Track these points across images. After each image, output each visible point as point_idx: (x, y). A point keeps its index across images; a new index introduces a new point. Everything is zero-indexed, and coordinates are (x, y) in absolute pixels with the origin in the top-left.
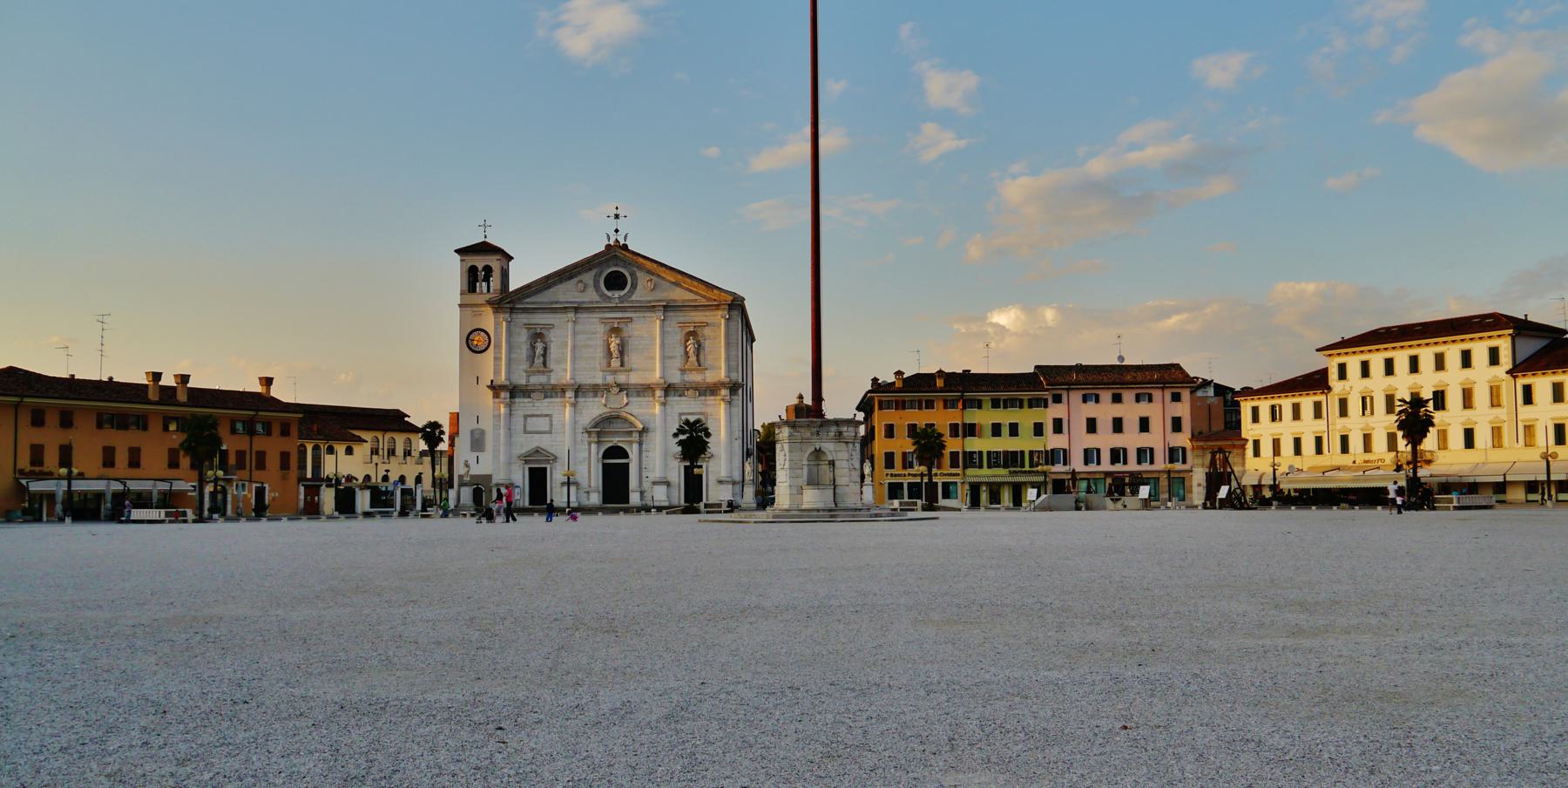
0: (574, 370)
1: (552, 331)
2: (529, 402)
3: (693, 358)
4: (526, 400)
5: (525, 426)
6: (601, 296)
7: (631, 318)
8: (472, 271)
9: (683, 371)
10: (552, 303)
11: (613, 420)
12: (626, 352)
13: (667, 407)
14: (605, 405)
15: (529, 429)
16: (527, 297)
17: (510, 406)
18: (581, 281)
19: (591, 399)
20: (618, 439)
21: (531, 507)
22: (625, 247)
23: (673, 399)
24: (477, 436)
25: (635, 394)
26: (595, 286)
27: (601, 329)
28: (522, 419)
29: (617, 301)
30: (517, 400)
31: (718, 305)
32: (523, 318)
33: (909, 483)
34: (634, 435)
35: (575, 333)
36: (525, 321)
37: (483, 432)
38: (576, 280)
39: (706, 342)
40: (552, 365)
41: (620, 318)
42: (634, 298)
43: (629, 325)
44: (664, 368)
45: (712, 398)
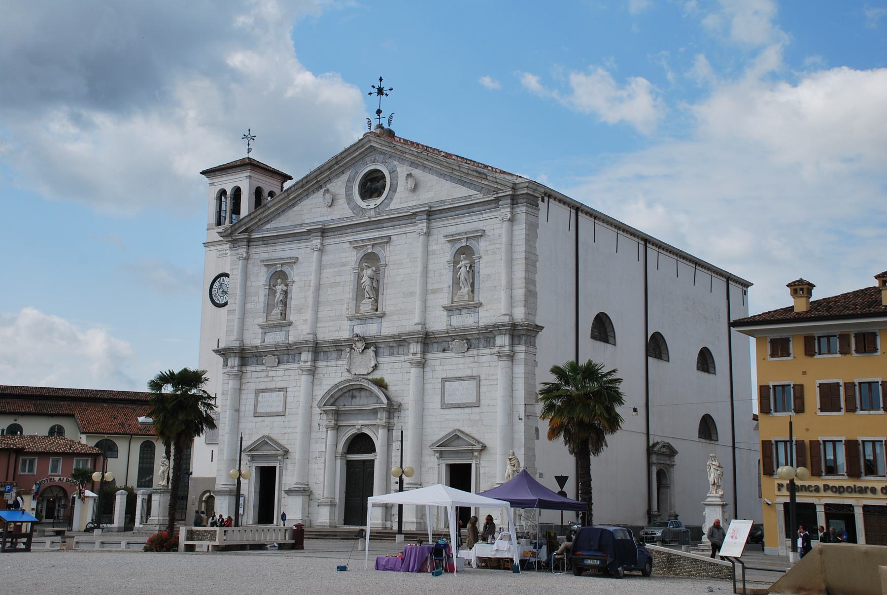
0: (316, 320)
1: (295, 266)
2: (263, 371)
3: (465, 290)
4: (259, 368)
5: (256, 406)
6: (353, 209)
7: (389, 237)
9: (449, 309)
10: (295, 226)
11: (356, 393)
12: (380, 290)
13: (427, 369)
14: (349, 371)
15: (260, 410)
16: (268, 222)
17: (240, 376)
18: (327, 191)
19: (334, 363)
20: (361, 422)
22: (391, 134)
23: (435, 357)
25: (387, 351)
26: (346, 196)
27: (352, 257)
28: (253, 396)
29: (372, 213)
30: (249, 368)
31: (498, 199)
32: (261, 253)
33: (826, 506)
34: (379, 415)
35: (320, 267)
36: (265, 256)
38: (322, 190)
39: (482, 261)
40: (292, 317)
41: (374, 239)
42: (392, 206)
43: (389, 248)
44: (425, 309)
45: (488, 351)
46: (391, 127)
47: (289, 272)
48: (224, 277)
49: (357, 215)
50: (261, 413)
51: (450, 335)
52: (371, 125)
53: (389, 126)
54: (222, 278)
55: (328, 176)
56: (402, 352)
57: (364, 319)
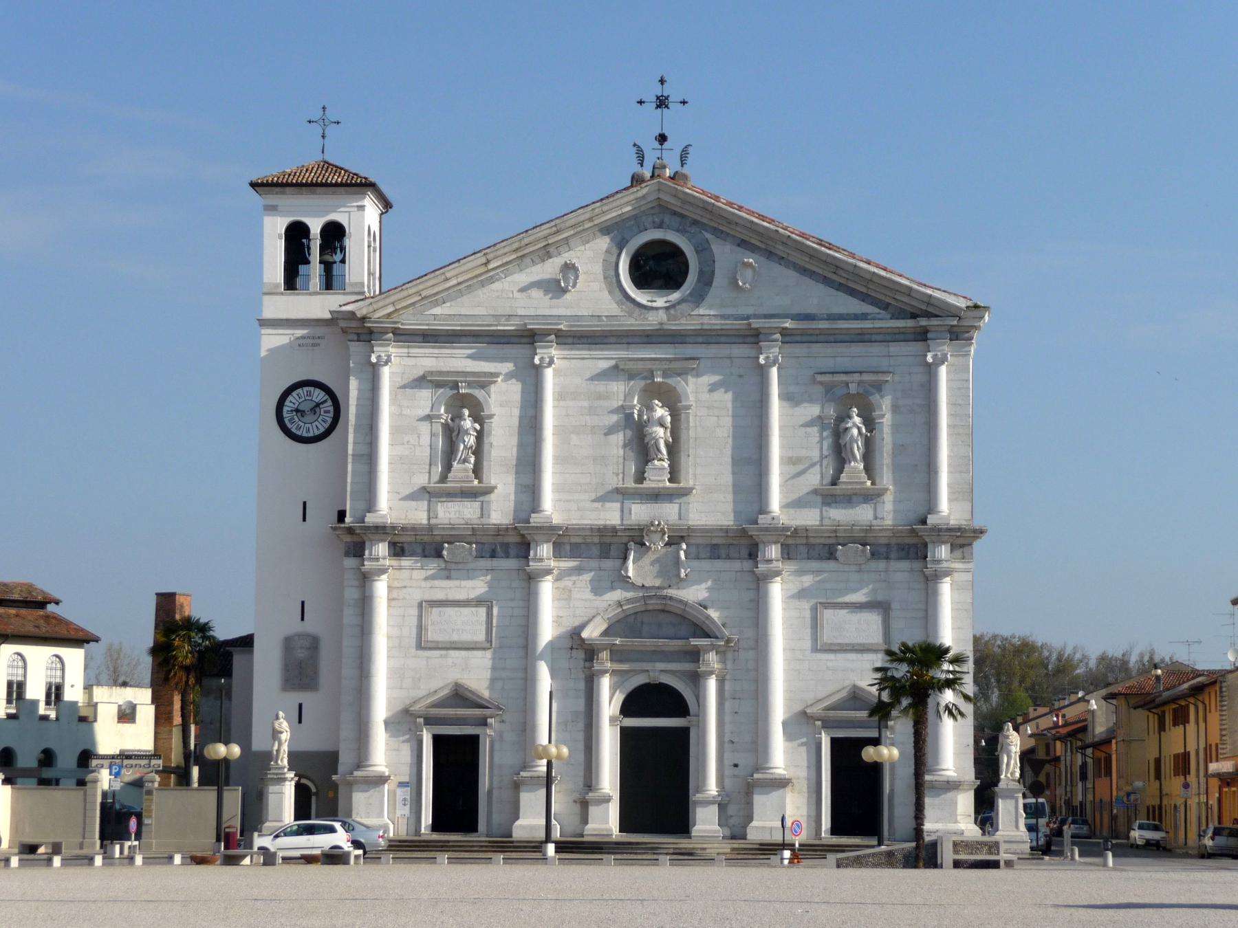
8: (296, 234)
15: (432, 635)
21: (436, 836)
24: (301, 654)
29: (662, 316)
37: (314, 644)
46: (685, 170)
47: (486, 398)
48: (312, 389)
49: (630, 314)
50: (438, 642)
51: (838, 535)
52: (643, 157)
53: (682, 166)
54: (306, 389)
55: (567, 238)
56: (737, 555)
57: (656, 496)
